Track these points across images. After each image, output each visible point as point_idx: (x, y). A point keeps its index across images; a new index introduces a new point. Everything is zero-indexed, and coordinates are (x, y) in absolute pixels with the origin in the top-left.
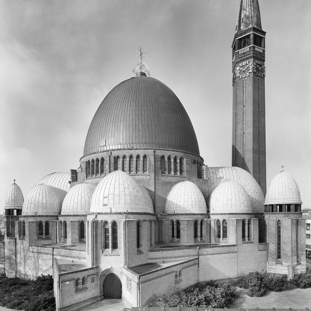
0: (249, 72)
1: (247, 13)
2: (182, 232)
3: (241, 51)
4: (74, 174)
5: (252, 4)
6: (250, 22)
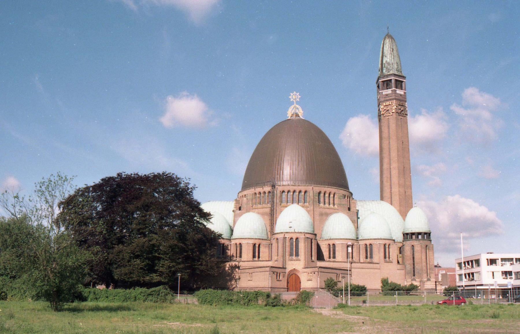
1: (388, 60)
2: (337, 253)
4: (237, 204)
5: (392, 53)
6: (391, 68)
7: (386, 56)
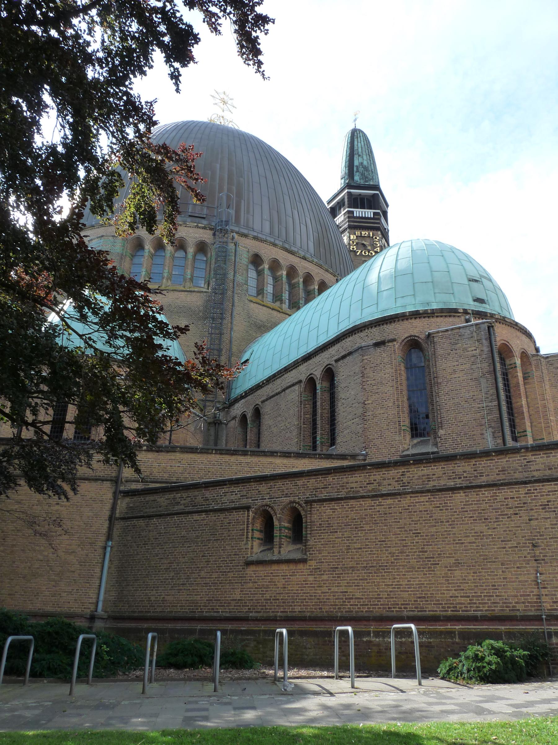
0: (375, 250)
3: (358, 212)
7: (359, 156)
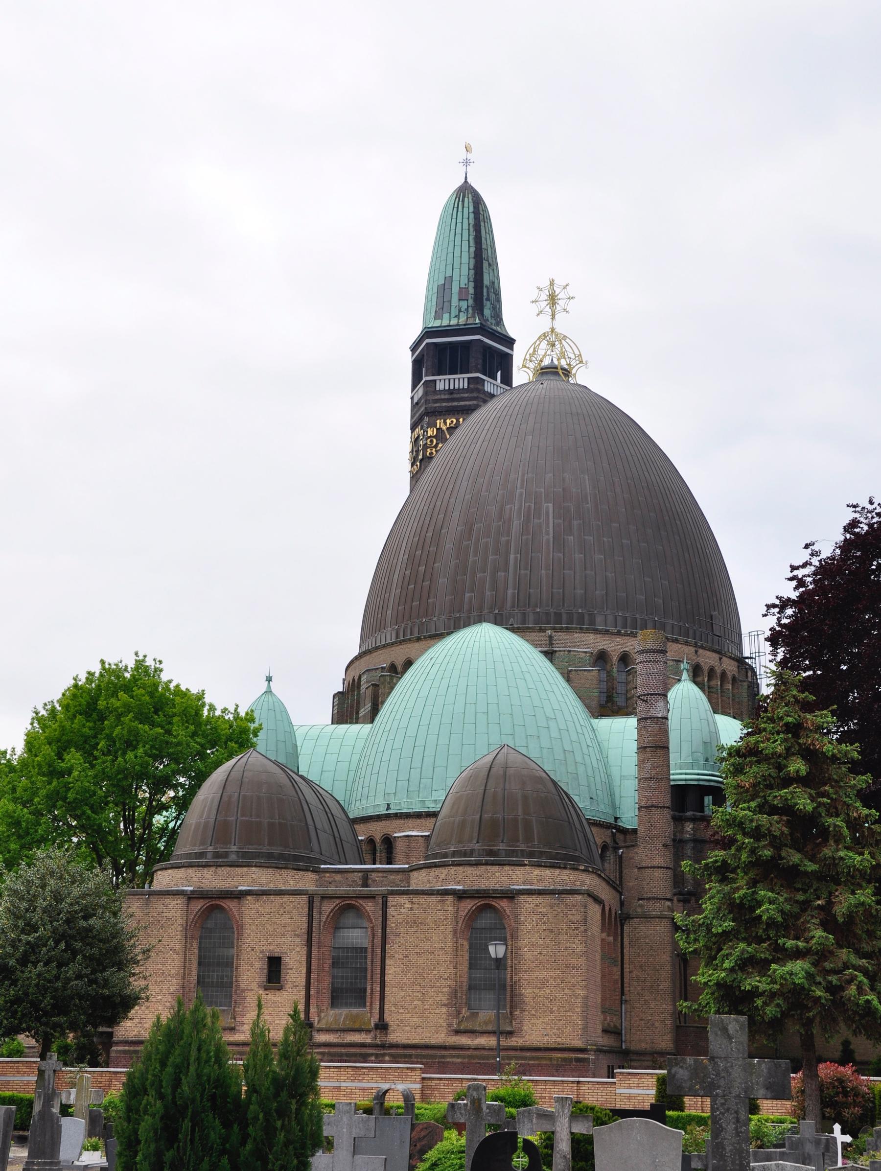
3: (443, 382)
